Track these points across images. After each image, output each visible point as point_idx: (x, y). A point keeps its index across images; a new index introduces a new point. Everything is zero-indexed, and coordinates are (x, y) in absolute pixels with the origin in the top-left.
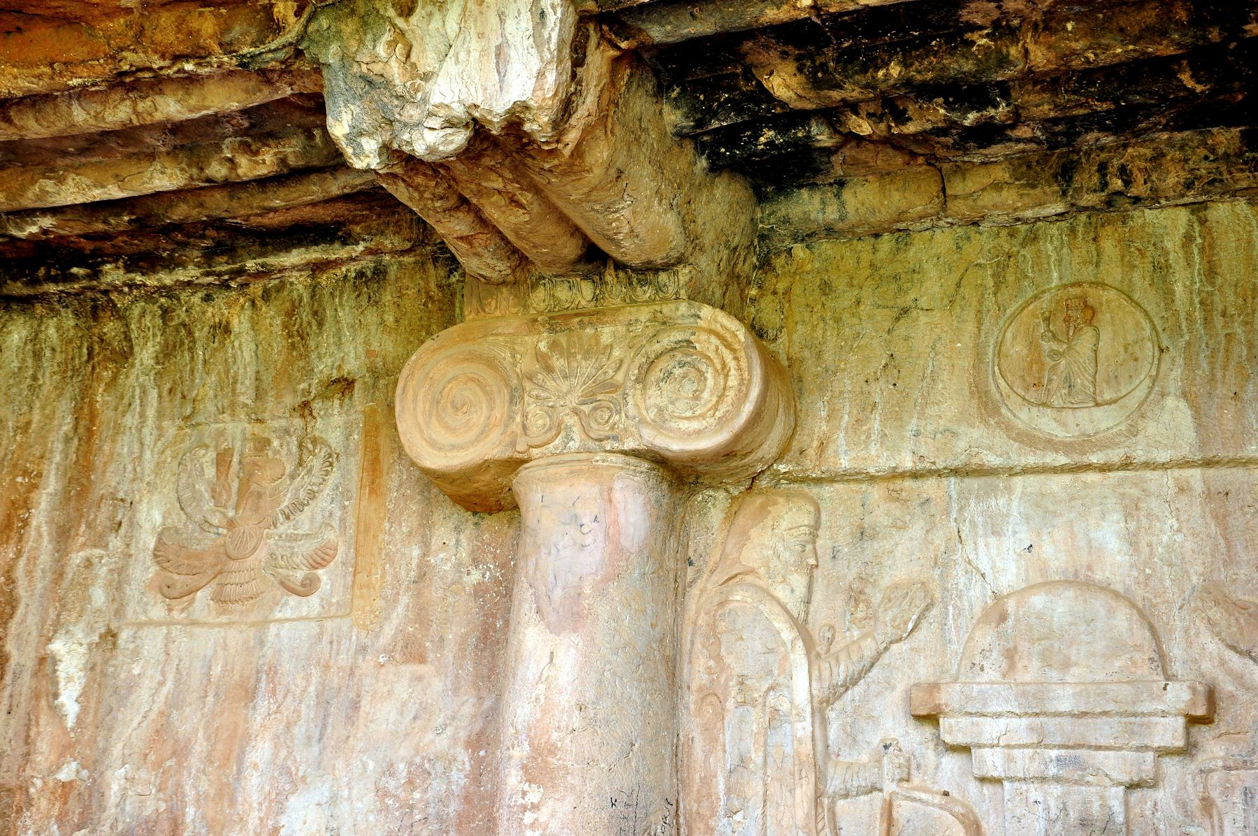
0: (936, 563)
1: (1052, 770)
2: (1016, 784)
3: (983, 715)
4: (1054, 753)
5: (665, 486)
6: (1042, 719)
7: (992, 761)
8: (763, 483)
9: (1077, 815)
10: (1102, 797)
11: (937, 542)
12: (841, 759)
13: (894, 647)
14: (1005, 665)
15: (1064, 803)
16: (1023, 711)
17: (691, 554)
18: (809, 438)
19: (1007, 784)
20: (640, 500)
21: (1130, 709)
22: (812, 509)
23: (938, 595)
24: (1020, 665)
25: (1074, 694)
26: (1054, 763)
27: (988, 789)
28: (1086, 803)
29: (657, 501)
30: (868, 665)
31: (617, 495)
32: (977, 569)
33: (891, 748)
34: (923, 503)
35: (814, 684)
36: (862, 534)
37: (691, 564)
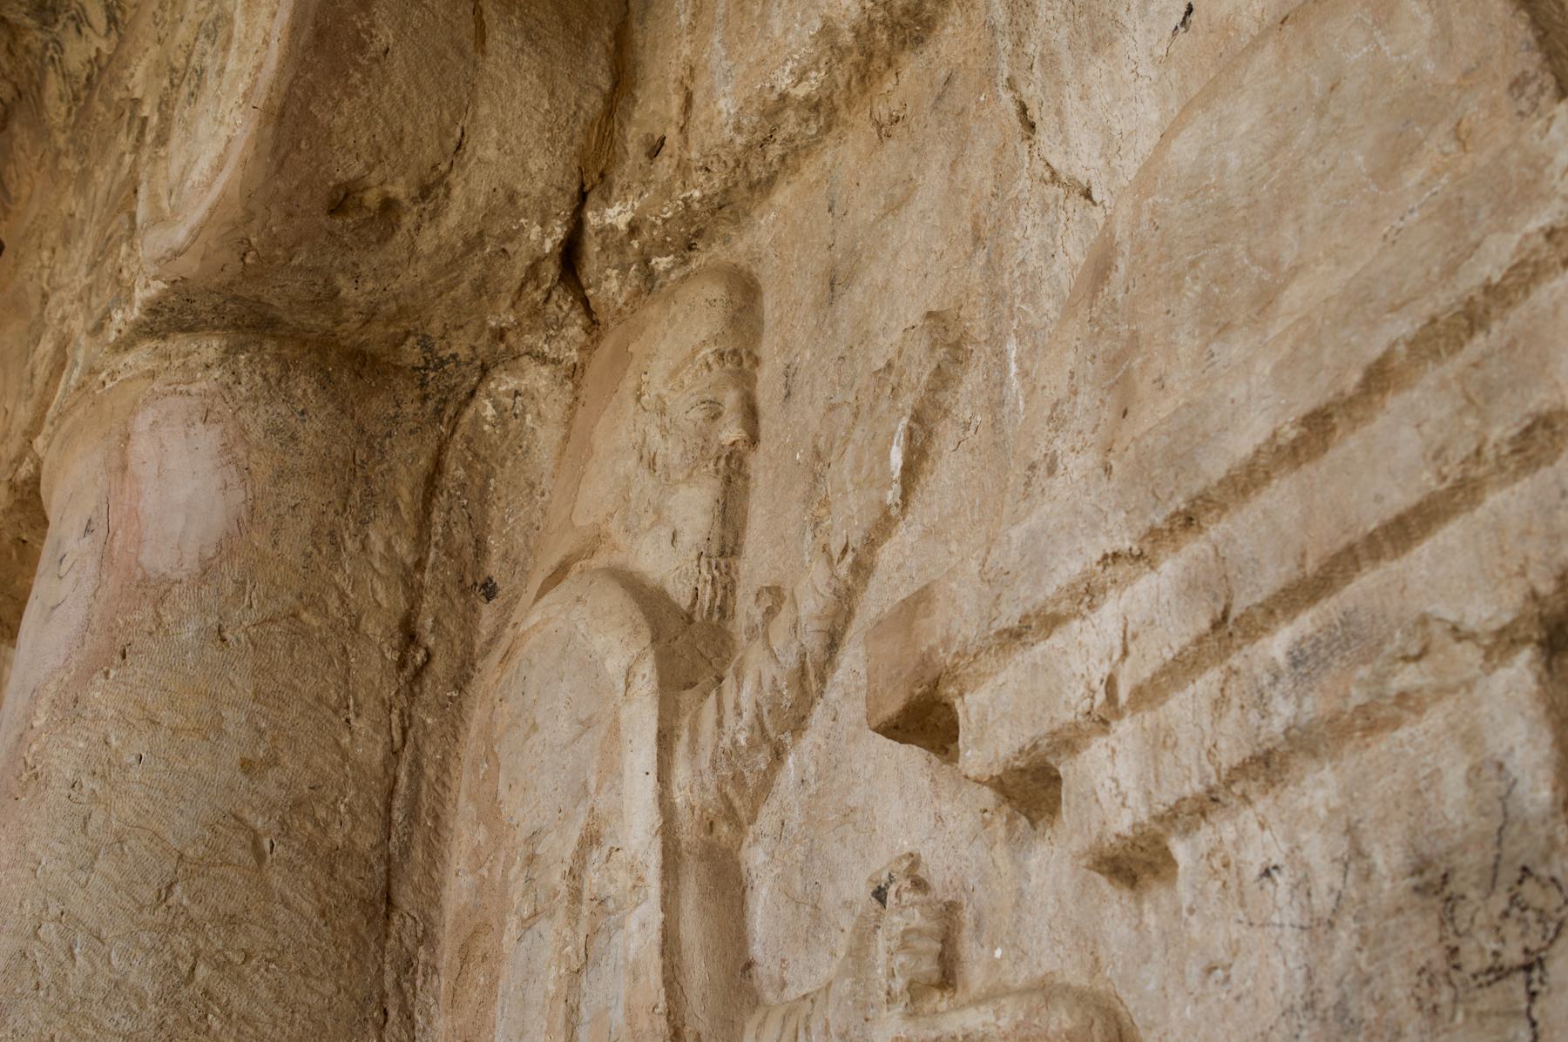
0: (977, 239)
1: (1283, 711)
2: (1205, 836)
3: (1053, 623)
4: (1278, 643)
5: (303, 386)
6: (1216, 530)
7: (1113, 785)
8: (609, 285)
9: (1398, 857)
10: (1470, 739)
11: (976, 174)
12: (792, 993)
13: (886, 554)
14: (1108, 414)
15: (1351, 830)
16: (1142, 526)
17: (494, 568)
18: (654, 108)
19: (1180, 850)
20: (209, 438)
21: (1443, 300)
22: (716, 291)
23: (978, 326)
24: (1144, 386)
25: (1278, 368)
26: (1286, 683)
27: (1154, 909)
28: (1420, 790)
29: (273, 430)
30: (814, 642)
31: (142, 447)
32: (1071, 185)
33: (893, 889)
34: (940, 98)
35: (681, 772)
36: (834, 284)
37: (489, 590)
